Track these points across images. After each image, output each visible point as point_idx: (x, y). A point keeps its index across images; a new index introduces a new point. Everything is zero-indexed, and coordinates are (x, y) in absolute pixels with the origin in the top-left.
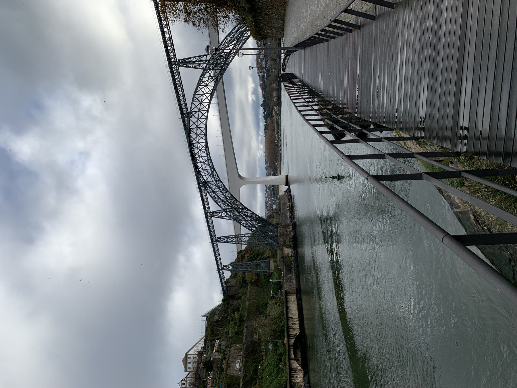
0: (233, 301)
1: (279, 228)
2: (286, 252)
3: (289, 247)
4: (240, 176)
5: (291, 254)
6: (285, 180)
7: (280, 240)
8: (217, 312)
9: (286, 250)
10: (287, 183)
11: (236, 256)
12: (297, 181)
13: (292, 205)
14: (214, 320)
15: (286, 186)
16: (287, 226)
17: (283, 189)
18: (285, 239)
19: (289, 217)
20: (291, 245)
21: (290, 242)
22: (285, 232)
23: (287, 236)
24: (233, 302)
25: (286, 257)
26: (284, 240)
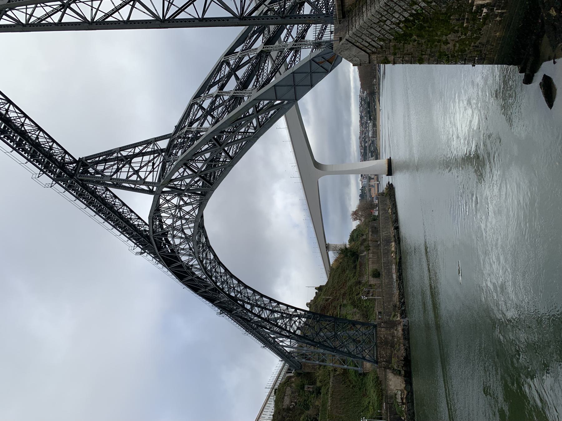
0: (309, 386)
1: (378, 329)
2: (392, 387)
3: (397, 373)
4: (317, 165)
5: (402, 399)
6: (387, 169)
7: (380, 354)
8: (288, 391)
9: (391, 380)
10: (390, 172)
11: (315, 295)
12: (407, 166)
13: (400, 258)
14: (284, 407)
15: (388, 175)
16: (392, 325)
17: (385, 180)
18: (390, 352)
19: (394, 276)
20: (400, 371)
21: (398, 366)
22: (390, 338)
23: (393, 346)
24: (309, 387)
25: (391, 397)
26: (388, 354)
